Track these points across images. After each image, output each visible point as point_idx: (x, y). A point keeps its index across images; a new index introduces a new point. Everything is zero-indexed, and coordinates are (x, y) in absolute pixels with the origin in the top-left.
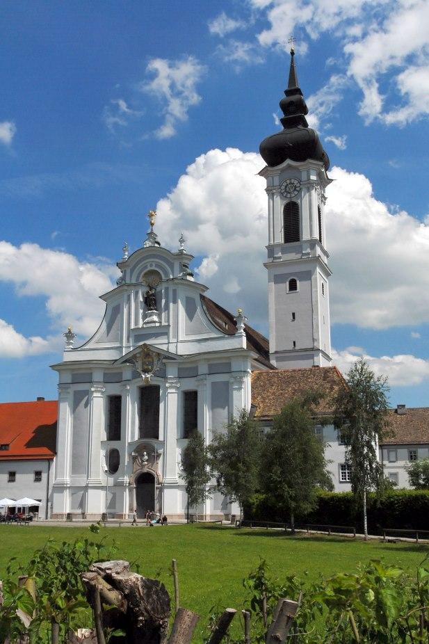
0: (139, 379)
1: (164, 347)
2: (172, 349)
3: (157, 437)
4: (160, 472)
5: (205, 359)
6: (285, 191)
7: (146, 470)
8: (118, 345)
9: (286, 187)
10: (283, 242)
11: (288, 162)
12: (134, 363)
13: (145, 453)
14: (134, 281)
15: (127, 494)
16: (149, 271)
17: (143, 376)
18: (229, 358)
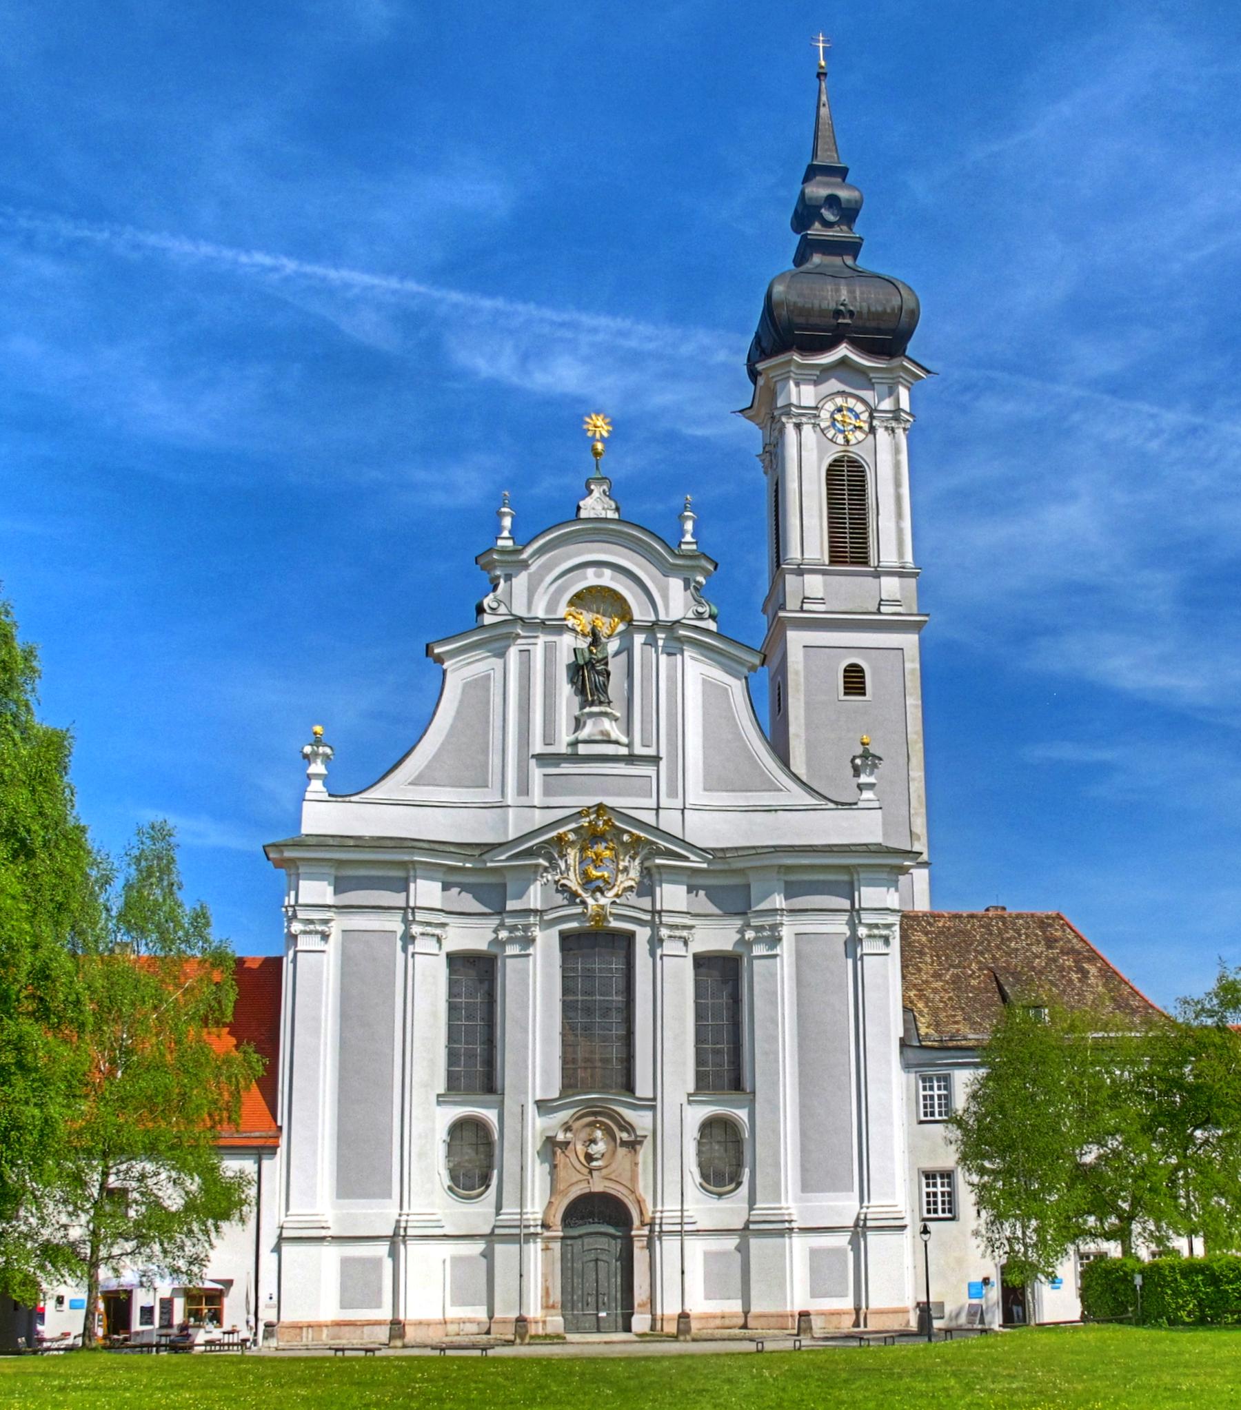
0: (579, 910)
1: (649, 818)
2: (670, 822)
3: (629, 1086)
4: (644, 1188)
5: (780, 866)
6: (833, 425)
7: (598, 1186)
8: (492, 797)
9: (832, 414)
10: (827, 562)
11: (843, 350)
12: (550, 859)
13: (599, 1134)
14: (540, 612)
15: (534, 1250)
16: (585, 589)
17: (590, 901)
18: (846, 868)
